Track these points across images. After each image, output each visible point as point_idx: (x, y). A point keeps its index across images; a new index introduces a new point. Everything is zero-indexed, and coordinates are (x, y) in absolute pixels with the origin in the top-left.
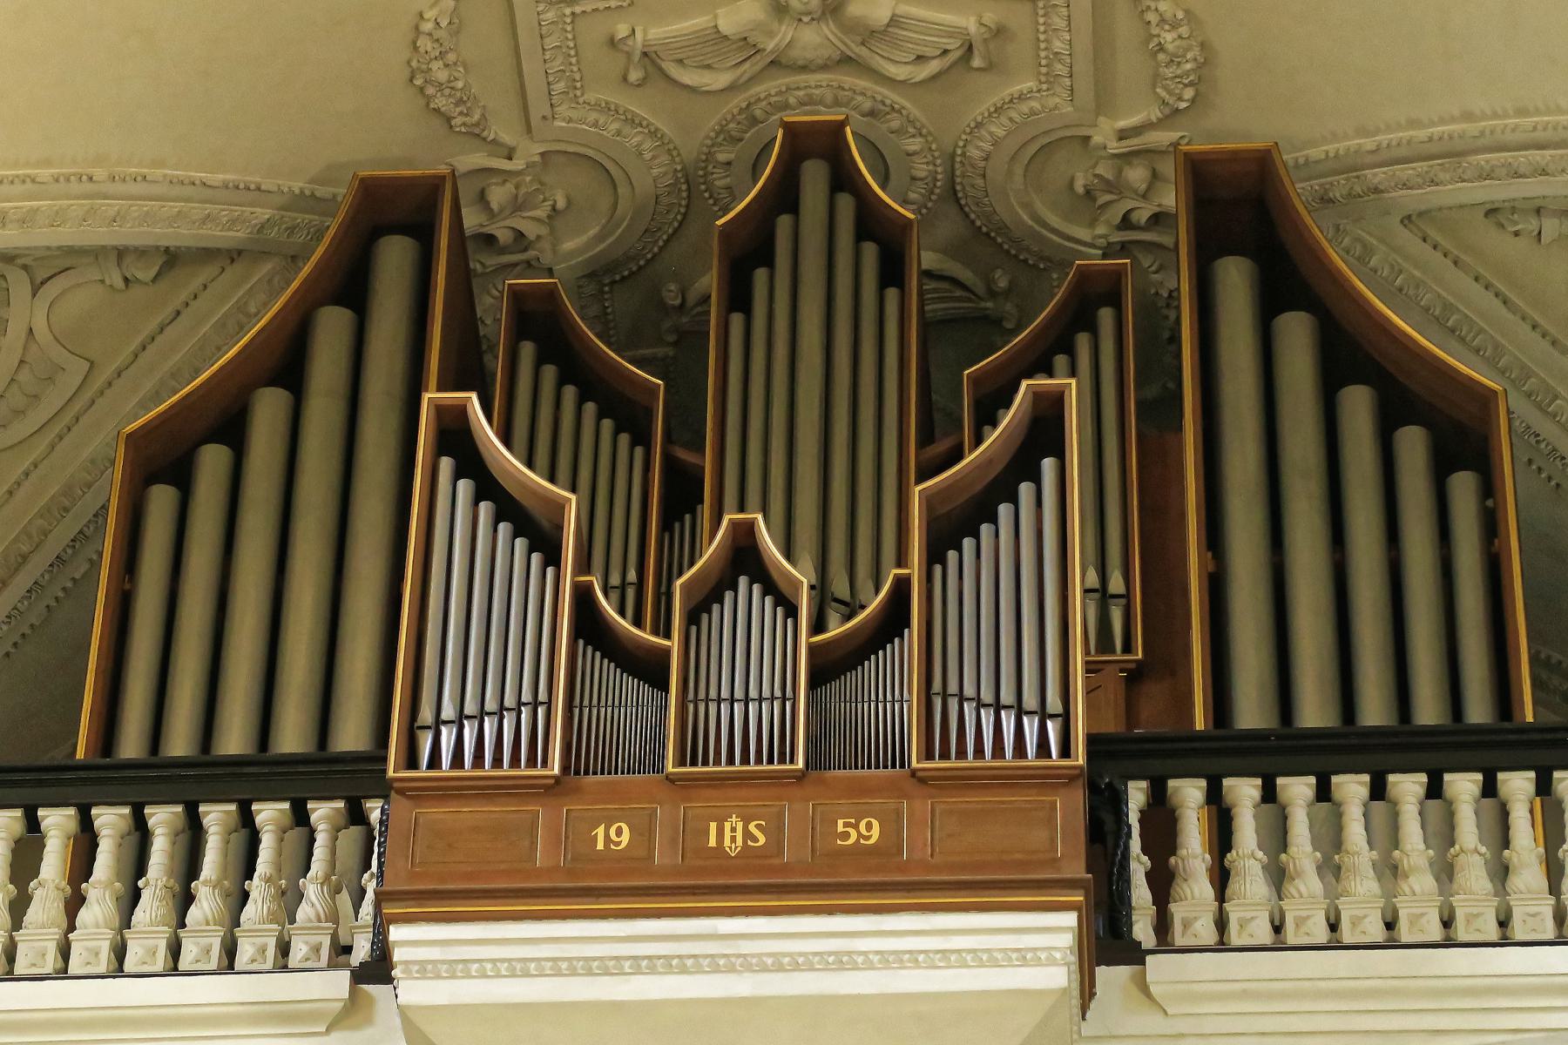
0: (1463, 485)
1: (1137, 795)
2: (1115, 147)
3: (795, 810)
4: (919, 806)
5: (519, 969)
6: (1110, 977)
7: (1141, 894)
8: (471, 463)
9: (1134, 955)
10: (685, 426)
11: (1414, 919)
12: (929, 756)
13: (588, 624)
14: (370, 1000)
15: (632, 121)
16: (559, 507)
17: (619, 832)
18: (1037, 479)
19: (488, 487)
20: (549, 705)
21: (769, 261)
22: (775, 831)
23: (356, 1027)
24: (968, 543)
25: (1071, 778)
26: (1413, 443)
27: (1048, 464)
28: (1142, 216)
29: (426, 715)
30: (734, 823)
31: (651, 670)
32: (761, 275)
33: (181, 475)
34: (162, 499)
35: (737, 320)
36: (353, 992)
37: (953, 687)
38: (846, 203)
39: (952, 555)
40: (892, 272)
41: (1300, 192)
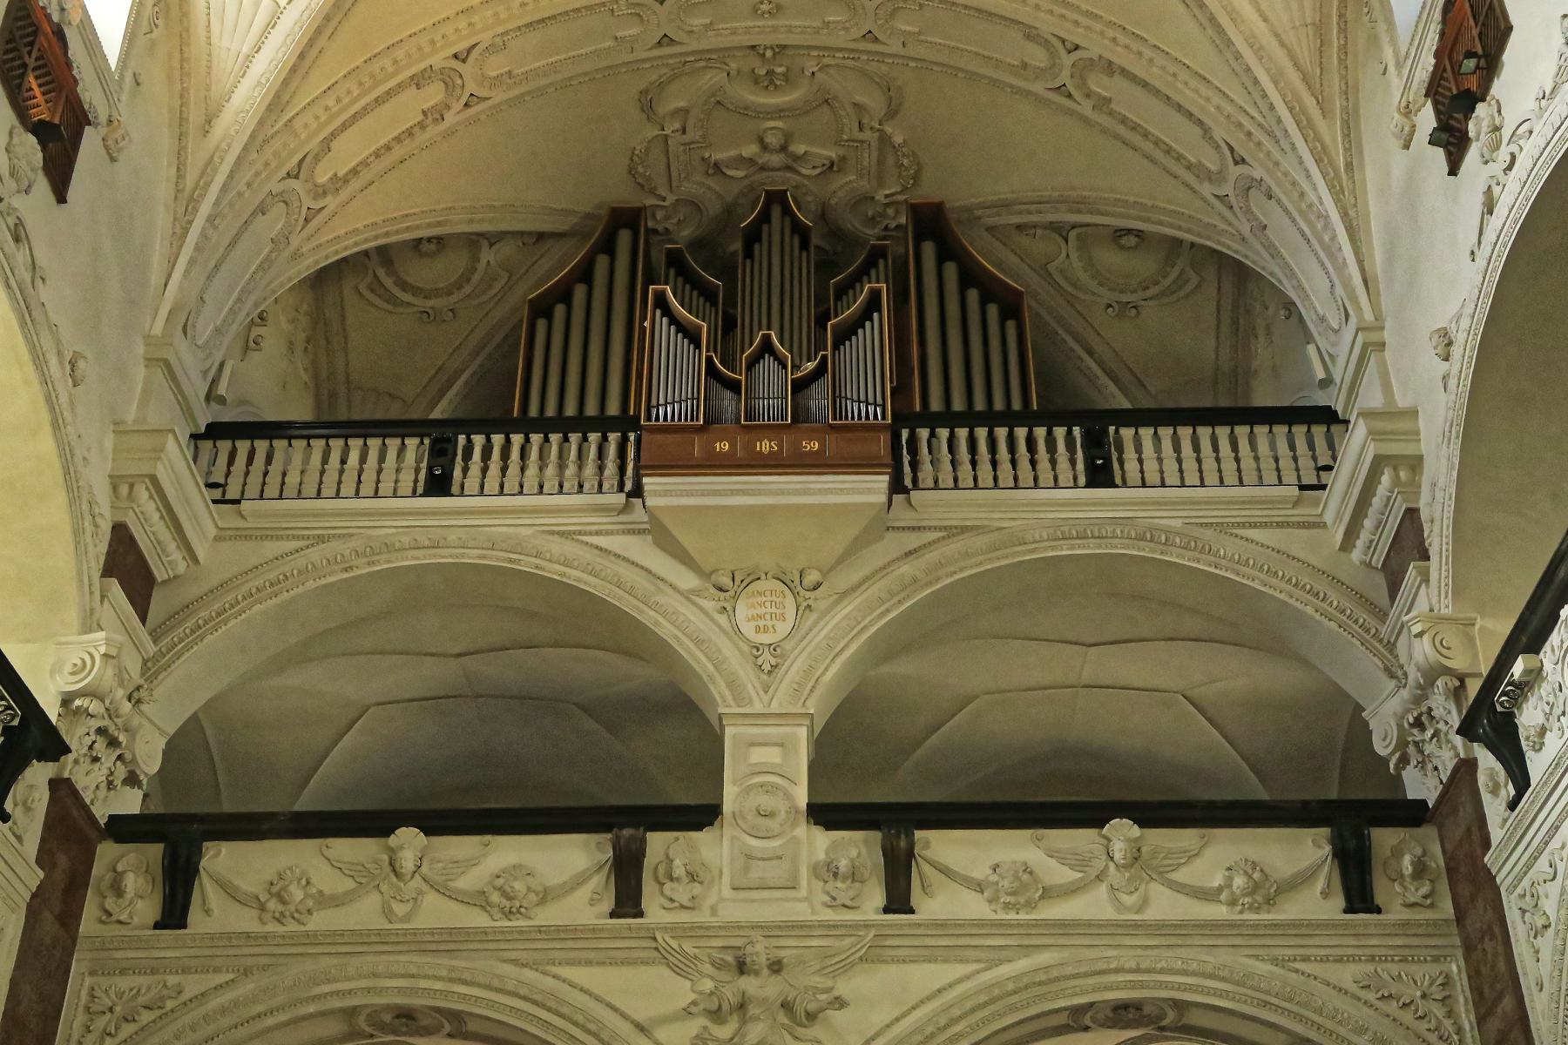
0: (1011, 326)
1: (905, 434)
2: (884, 201)
4: (831, 439)
5: (689, 494)
6: (897, 498)
7: (907, 469)
9: (906, 491)
10: (731, 301)
11: (983, 480)
12: (835, 419)
13: (711, 370)
14: (632, 502)
15: (709, 188)
16: (700, 328)
18: (871, 320)
19: (674, 320)
20: (698, 399)
21: (759, 240)
23: (628, 513)
24: (847, 343)
26: (993, 310)
27: (876, 315)
28: (893, 225)
29: (654, 402)
31: (734, 387)
32: (757, 246)
33: (549, 315)
34: (541, 325)
35: (748, 262)
37: (843, 395)
39: (842, 347)
40: (805, 245)
41: (952, 217)
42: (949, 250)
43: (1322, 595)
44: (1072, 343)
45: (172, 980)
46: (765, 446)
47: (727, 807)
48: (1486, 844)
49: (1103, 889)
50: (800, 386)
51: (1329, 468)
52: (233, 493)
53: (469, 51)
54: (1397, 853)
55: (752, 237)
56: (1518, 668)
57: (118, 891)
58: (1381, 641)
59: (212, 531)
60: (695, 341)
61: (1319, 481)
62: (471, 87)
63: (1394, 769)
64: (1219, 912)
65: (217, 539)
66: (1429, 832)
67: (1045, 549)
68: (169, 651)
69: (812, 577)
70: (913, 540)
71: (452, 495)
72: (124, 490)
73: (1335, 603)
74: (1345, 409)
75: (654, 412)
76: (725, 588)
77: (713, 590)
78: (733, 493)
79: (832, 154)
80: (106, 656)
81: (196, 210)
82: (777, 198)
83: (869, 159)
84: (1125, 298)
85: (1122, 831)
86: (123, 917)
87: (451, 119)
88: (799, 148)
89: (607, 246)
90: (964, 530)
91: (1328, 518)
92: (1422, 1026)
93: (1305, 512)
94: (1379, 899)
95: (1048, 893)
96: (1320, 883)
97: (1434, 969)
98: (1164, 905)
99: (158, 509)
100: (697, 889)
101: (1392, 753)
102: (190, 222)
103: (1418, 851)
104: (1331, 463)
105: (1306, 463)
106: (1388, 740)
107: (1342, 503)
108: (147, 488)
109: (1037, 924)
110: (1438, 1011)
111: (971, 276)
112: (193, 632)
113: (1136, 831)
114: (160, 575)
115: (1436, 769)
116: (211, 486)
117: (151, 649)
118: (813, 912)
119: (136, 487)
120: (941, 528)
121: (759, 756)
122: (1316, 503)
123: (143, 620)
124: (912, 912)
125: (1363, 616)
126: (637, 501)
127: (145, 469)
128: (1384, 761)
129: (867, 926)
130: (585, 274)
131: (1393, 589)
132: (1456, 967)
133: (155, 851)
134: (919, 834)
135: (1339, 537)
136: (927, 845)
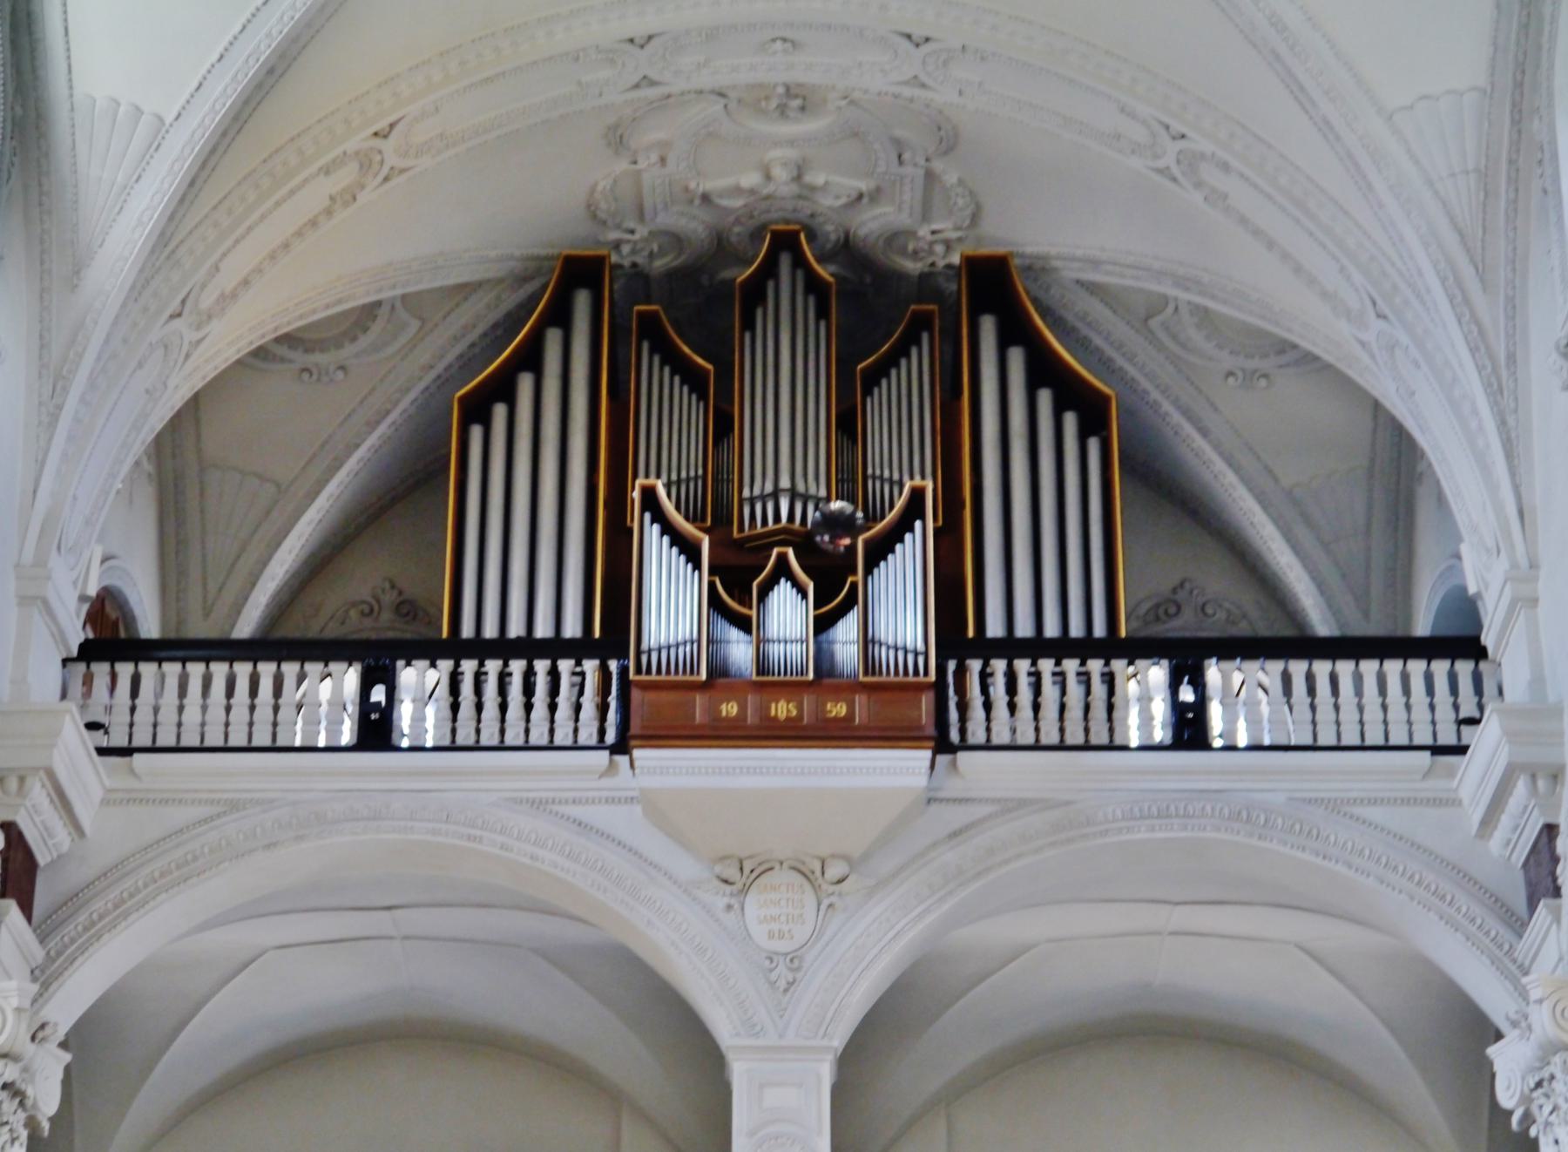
0: (1094, 445)
1: (952, 665)
2: (929, 237)
3: (807, 701)
6: (942, 759)
7: (953, 715)
8: (659, 517)
13: (715, 603)
17: (732, 707)
19: (668, 528)
21: (761, 298)
22: (800, 708)
25: (928, 686)
26: (1070, 420)
29: (645, 646)
31: (744, 624)
32: (759, 312)
34: (476, 432)
36: (611, 761)
38: (800, 274)
42: (1016, 330)
43: (1449, 898)
44: (1176, 418)
46: (782, 709)
50: (823, 624)
51: (1473, 722)
52: (119, 740)
53: (392, 126)
55: (754, 293)
58: (1514, 961)
59: (97, 794)
60: (693, 556)
61: (1459, 738)
62: (392, 160)
63: (1521, 1122)
65: (105, 802)
67: (1120, 831)
68: (59, 954)
69: (834, 871)
70: (958, 816)
71: (399, 749)
73: (1464, 909)
74: (1497, 645)
75: (644, 659)
76: (731, 880)
77: (717, 883)
79: (863, 185)
80: (18, 1010)
81: (65, 390)
82: (785, 241)
83: (911, 195)
87: (363, 198)
88: (817, 178)
89: (559, 315)
90: (1022, 804)
91: (1465, 794)
93: (1434, 786)
99: (49, 795)
101: (1518, 1105)
102: (60, 407)
104: (1476, 715)
105: (1445, 714)
106: (1512, 1090)
107: (1480, 785)
108: (41, 780)
112: (86, 929)
114: (42, 858)
115: (1557, 1142)
116: (92, 726)
117: (39, 954)
119: (29, 781)
123: (29, 918)
125: (1496, 927)
126: (622, 760)
128: (1510, 1113)
131: (1532, 906)
135: (1477, 816)
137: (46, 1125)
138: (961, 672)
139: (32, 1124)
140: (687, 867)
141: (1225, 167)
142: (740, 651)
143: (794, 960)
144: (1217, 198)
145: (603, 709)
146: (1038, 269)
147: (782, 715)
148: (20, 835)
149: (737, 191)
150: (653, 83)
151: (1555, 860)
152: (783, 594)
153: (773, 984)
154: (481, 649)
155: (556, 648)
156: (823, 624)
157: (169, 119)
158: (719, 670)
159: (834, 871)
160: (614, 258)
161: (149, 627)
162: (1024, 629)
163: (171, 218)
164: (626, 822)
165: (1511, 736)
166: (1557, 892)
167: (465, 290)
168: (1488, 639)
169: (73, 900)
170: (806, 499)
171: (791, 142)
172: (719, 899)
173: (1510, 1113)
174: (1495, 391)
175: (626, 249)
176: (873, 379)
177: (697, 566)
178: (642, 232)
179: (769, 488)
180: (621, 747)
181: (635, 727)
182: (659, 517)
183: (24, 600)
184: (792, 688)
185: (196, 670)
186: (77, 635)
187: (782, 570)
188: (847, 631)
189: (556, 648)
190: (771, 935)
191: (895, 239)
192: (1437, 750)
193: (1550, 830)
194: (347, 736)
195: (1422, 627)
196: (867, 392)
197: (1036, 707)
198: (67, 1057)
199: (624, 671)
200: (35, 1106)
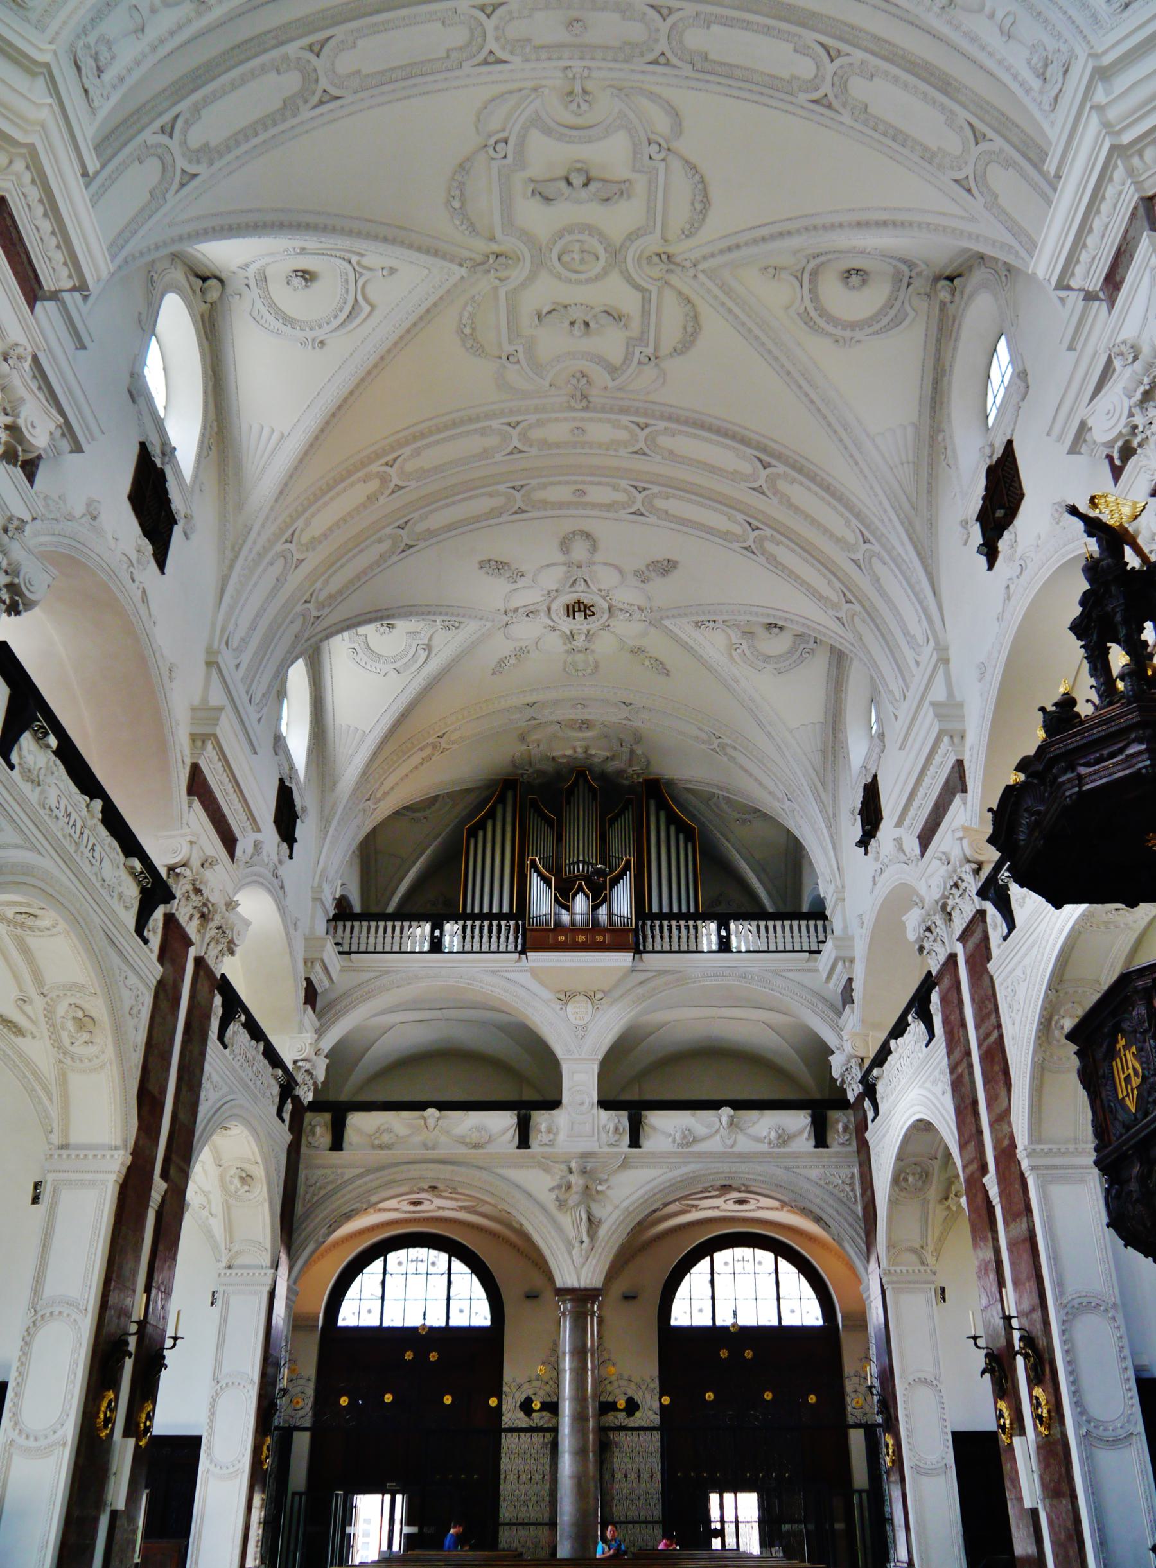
1: (640, 923)
6: (637, 956)
9: (640, 952)
13: (556, 900)
19: (540, 874)
22: (587, 938)
26: (681, 836)
30: (580, 940)
31: (567, 908)
42: (662, 805)
44: (719, 835)
45: (339, 1171)
46: (580, 938)
47: (564, 1101)
48: (866, 1128)
49: (718, 1137)
50: (595, 908)
51: (823, 942)
52: (346, 948)
54: (837, 1121)
55: (571, 791)
56: (875, 1072)
57: (314, 1134)
59: (339, 968)
60: (549, 885)
62: (444, 746)
64: (764, 1147)
66: (850, 1112)
67: (700, 982)
69: (599, 996)
72: (309, 964)
78: (566, 960)
79: (608, 754)
82: (581, 774)
83: (625, 757)
84: (746, 816)
85: (726, 1112)
86: (316, 1144)
87: (434, 759)
88: (593, 752)
89: (502, 800)
90: (666, 972)
91: (820, 968)
92: (842, 1195)
93: (811, 964)
94: (829, 1141)
95: (696, 1140)
96: (806, 1135)
97: (847, 1171)
98: (743, 1144)
100: (551, 1136)
102: (327, 832)
103: (846, 1121)
105: (813, 939)
109: (690, 1153)
110: (848, 1189)
111: (672, 819)
113: (732, 1112)
114: (319, 991)
116: (337, 944)
117: (317, 1024)
118: (600, 1147)
120: (656, 971)
121: (577, 1077)
122: (816, 960)
124: (640, 1147)
125: (832, 1014)
126: (524, 956)
127: (317, 955)
128: (837, 1080)
129: (621, 1154)
130: (491, 815)
131: (844, 1008)
132: (856, 1170)
133: (327, 1116)
134: (644, 1113)
135: (825, 975)
136: (649, 1117)
137: (320, 1085)
138: (644, 925)
139: (315, 1084)
140: (547, 995)
141: (735, 748)
142: (565, 918)
143: (584, 1028)
144: (732, 759)
145: (516, 938)
146: (670, 783)
147: (580, 940)
148: (312, 982)
149: (564, 756)
150: (535, 719)
151: (852, 990)
152: (581, 899)
153: (577, 1036)
154: (473, 917)
155: (500, 916)
156: (595, 908)
157: (367, 732)
158: (558, 924)
159: (599, 996)
160: (521, 780)
161: (357, 909)
162: (666, 910)
163: (367, 766)
164: (525, 978)
165: (836, 947)
166: (853, 1002)
167: (468, 791)
168: (828, 913)
169: (330, 1005)
170: (588, 864)
171: (583, 739)
172: (558, 1006)
173: (837, 1080)
174: (829, 826)
175: (525, 776)
176: (612, 822)
177: (550, 888)
178: (531, 770)
179: (575, 860)
180: (523, 952)
181: (528, 945)
182: (537, 870)
183: (315, 899)
184: (583, 931)
185: (373, 924)
186: (332, 912)
187: (580, 889)
188: (603, 911)
189: (500, 916)
190: (576, 1019)
191: (621, 772)
192: (811, 952)
193: (850, 980)
194: (426, 947)
195: (805, 908)
196: (610, 826)
197: (670, 937)
198: (328, 1061)
199: (524, 925)
200: (316, 1078)
